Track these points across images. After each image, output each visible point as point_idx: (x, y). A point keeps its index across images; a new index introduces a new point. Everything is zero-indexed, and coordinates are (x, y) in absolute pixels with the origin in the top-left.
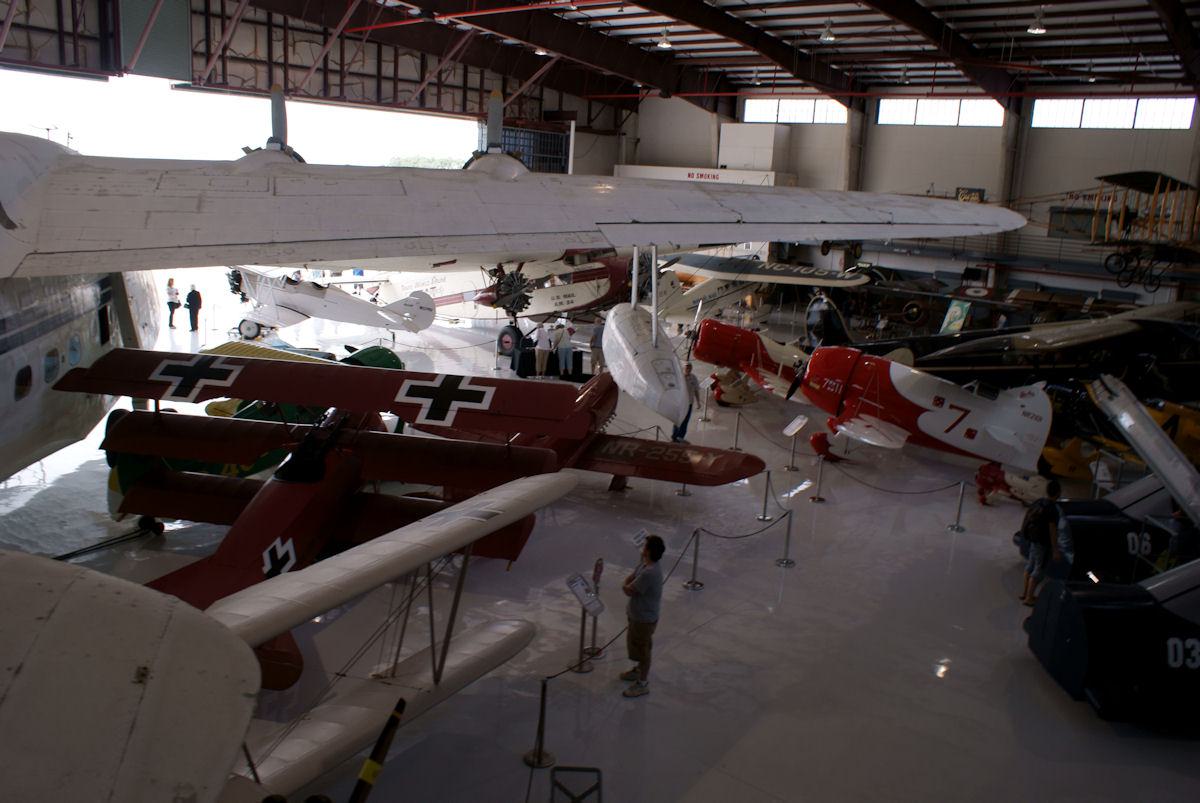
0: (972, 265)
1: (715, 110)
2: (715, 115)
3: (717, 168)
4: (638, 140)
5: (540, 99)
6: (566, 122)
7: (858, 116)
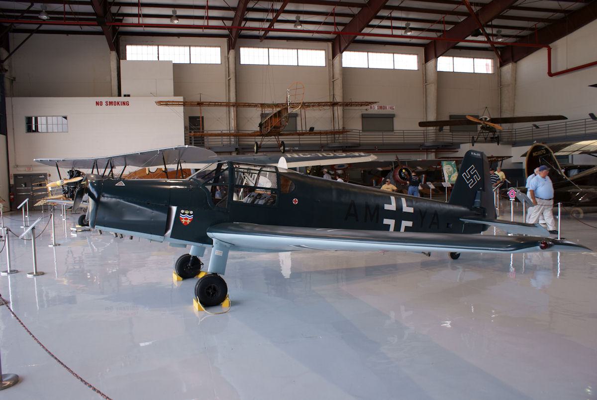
4: (14, 78)
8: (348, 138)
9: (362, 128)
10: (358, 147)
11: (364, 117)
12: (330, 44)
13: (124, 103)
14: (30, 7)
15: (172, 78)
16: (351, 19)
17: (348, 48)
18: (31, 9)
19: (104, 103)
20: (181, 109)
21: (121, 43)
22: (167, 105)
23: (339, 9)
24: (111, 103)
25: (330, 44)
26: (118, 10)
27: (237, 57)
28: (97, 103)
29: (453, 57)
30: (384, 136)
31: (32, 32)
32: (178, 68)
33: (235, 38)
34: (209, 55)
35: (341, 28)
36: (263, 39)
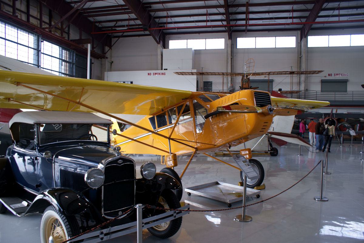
1: (158, 43)
4: (113, 62)
5: (68, 34)
6: (85, 45)
11: (323, 82)
12: (299, 32)
13: (163, 74)
14: (115, 24)
16: (319, 15)
17: (308, 34)
18: (116, 25)
19: (152, 74)
20: (195, 77)
21: (166, 39)
22: (183, 74)
23: (296, 7)
24: (156, 74)
25: (299, 32)
26: (159, 21)
27: (233, 45)
28: (149, 74)
29: (276, 37)
30: (336, 96)
31: (119, 37)
32: (197, 53)
33: (232, 32)
34: (218, 43)
35: (304, 20)
36: (247, 31)
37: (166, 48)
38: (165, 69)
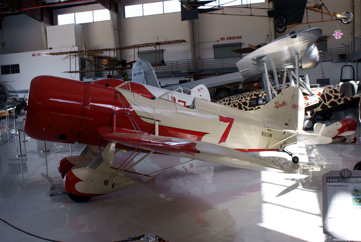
0: (183, 79)
1: (42, 20)
2: (42, 23)
3: (47, 49)
7: (115, 15)
8: (204, 66)
9: (215, 56)
10: (200, 72)
15: (74, 34)
28: (33, 55)
37: (54, 24)
38: (50, 49)
